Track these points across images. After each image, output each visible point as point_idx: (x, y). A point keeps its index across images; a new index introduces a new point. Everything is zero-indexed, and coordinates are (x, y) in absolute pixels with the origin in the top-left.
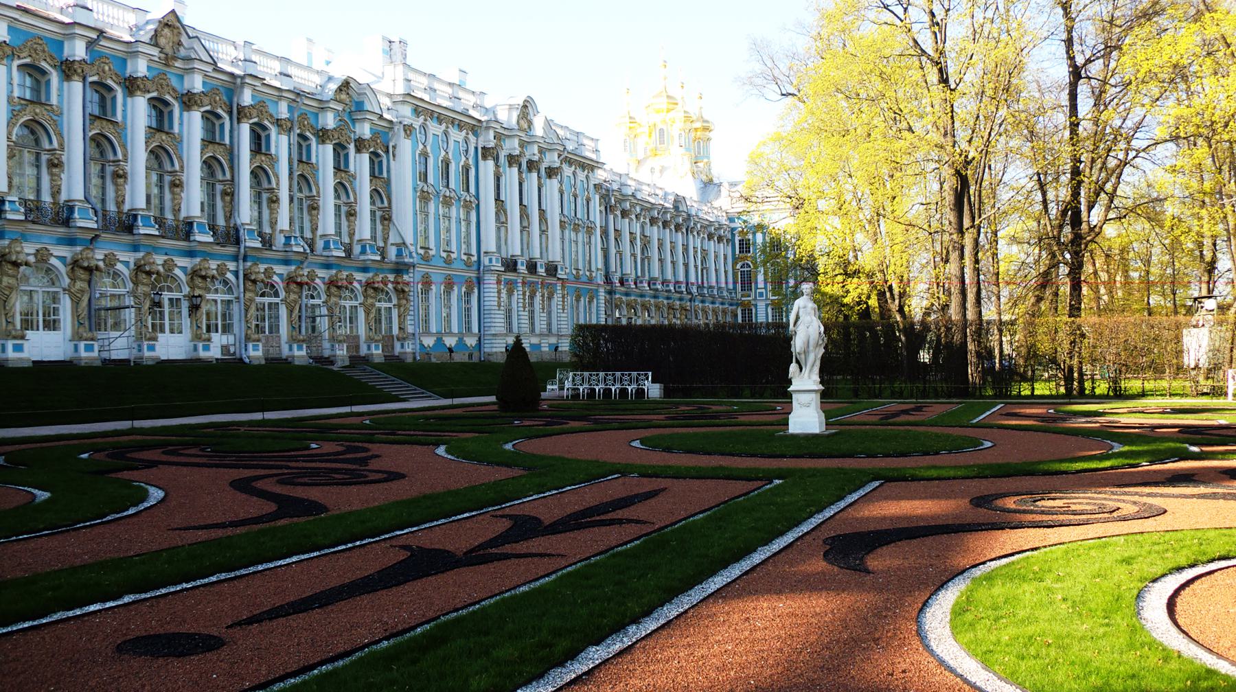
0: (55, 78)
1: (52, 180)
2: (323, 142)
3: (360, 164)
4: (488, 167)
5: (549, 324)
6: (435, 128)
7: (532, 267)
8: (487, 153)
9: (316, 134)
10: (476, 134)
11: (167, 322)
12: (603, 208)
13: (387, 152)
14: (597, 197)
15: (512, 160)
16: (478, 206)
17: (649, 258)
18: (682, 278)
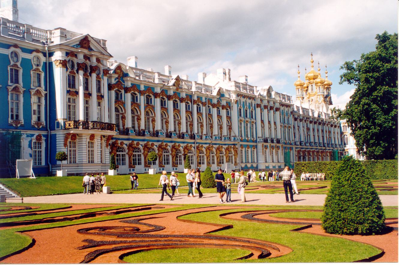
0: (153, 97)
1: (153, 125)
2: (214, 108)
3: (224, 113)
4: (258, 110)
5: (278, 160)
6: (243, 100)
7: (272, 141)
8: (258, 106)
9: (212, 105)
10: (254, 100)
11: (179, 162)
12: (294, 119)
13: (230, 108)
14: (292, 116)
15: (266, 107)
16: (256, 123)
17: (310, 135)
18: (321, 141)
